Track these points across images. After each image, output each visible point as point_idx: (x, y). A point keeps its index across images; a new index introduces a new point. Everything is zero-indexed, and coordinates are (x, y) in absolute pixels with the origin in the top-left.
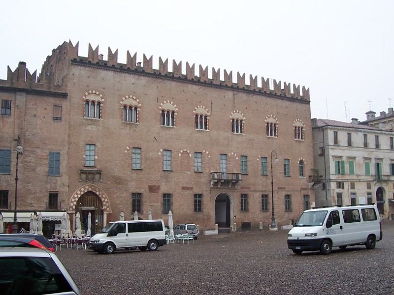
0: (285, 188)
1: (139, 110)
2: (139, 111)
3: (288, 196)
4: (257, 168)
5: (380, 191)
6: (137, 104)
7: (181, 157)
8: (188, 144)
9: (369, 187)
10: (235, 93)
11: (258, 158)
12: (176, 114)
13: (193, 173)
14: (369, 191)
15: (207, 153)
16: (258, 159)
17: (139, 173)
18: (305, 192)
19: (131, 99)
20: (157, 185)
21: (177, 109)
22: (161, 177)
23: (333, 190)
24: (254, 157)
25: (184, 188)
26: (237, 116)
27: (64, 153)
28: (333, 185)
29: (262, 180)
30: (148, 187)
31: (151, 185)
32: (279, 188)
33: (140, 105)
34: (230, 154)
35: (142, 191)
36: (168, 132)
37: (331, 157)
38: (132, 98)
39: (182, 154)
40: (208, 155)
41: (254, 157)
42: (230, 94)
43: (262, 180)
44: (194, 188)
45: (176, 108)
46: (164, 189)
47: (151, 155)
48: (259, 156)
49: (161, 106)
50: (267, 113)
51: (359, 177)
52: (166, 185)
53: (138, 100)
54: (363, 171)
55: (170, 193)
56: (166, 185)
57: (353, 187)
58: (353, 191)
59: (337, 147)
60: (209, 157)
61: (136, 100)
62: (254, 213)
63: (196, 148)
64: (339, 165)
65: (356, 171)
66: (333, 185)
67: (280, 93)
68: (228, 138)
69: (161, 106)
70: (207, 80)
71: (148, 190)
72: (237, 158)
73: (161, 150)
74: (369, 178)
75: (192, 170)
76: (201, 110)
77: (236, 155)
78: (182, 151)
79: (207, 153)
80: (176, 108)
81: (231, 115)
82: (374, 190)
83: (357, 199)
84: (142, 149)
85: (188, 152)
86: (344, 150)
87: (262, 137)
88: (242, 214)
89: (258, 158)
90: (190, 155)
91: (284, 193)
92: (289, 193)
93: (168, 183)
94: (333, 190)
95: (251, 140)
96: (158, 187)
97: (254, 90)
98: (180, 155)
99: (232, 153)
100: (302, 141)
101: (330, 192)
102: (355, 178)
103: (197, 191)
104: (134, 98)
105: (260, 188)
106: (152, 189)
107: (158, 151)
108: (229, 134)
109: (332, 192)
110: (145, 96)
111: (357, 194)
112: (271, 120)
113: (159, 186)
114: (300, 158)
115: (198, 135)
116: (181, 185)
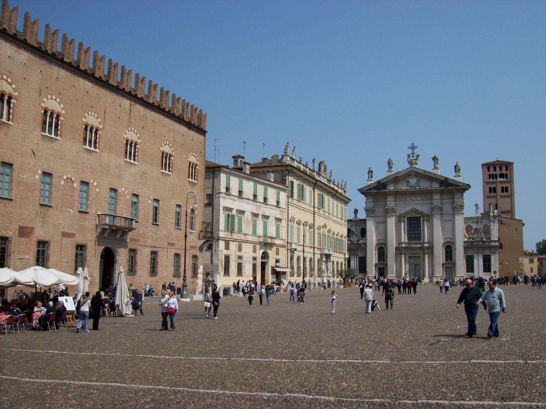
1: (15, 101)
2: (14, 103)
4: (149, 213)
5: (265, 256)
6: (12, 92)
7: (64, 185)
8: (73, 168)
9: (255, 251)
11: (150, 199)
12: (62, 118)
13: (78, 213)
14: (255, 255)
15: (95, 184)
17: (7, 205)
19: (4, 82)
20: (29, 225)
21: (64, 112)
22: (37, 214)
23: (222, 251)
24: (146, 197)
25: (64, 235)
26: (132, 136)
28: (222, 244)
29: (152, 231)
30: (18, 227)
31: (24, 225)
33: (16, 94)
34: (120, 190)
35: (9, 234)
36: (50, 145)
37: (221, 208)
38: (6, 80)
39: (65, 181)
40: (97, 186)
41: (146, 197)
43: (152, 231)
44: (77, 235)
45: (62, 109)
46: (40, 234)
47: (25, 177)
48: (152, 197)
49: (44, 102)
51: (247, 236)
52: (42, 227)
53: (14, 86)
54: (250, 231)
55: (47, 239)
56: (42, 227)
57: (240, 249)
58: (239, 254)
59: (228, 197)
60: (97, 190)
61: (10, 84)
62: (142, 276)
63: (82, 176)
64: (230, 219)
65: (244, 230)
66: (222, 244)
68: (120, 165)
69: (44, 102)
70: (102, 77)
71: (17, 233)
72: (128, 197)
73: (40, 172)
74: (255, 239)
75: (76, 208)
76: (92, 120)
77: (127, 192)
78: (65, 177)
79: (95, 184)
80: (62, 109)
81: (126, 133)
82: (259, 253)
83: (243, 264)
84: (14, 167)
85: (73, 179)
86: (235, 200)
87: (156, 170)
88: (128, 277)
89: (150, 199)
90: (75, 185)
91: (173, 251)
93: (45, 225)
94: (222, 251)
95: (144, 173)
96: (32, 229)
97: (153, 103)
98: (63, 182)
99: (123, 189)
101: (218, 254)
102: (243, 237)
103: (80, 240)
104: (9, 80)
105: (150, 242)
106: (24, 232)
107: (35, 173)
108: (121, 160)
109: (220, 254)
110: (24, 81)
111: (244, 258)
112: (167, 149)
113: (34, 228)
115: (85, 155)
116: (62, 230)
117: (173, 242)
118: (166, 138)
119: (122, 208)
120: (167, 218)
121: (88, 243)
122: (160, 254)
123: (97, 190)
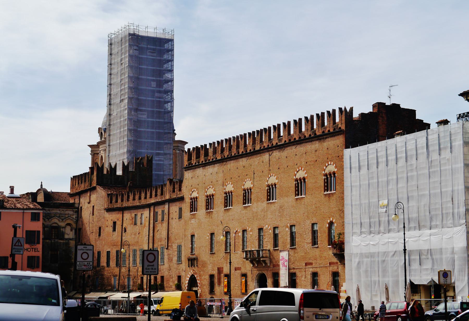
0: (311, 264)
3: (315, 275)
10: (271, 153)
15: (250, 229)
16: (287, 229)
18: (334, 268)
20: (221, 266)
24: (284, 226)
26: (273, 180)
27: (183, 244)
32: (306, 264)
34: (265, 228)
40: (251, 231)
41: (284, 226)
42: (266, 157)
44: (242, 268)
48: (288, 225)
50: (296, 166)
60: (251, 233)
67: (309, 133)
79: (250, 229)
89: (287, 226)
91: (310, 270)
92: (315, 270)
96: (223, 268)
99: (267, 226)
100: (332, 194)
103: (243, 271)
108: (265, 204)
114: (330, 218)
115: (244, 211)
117: (311, 261)
118: (298, 165)
119: (267, 241)
120: (304, 239)
121: (248, 272)
122: (298, 274)
123: (251, 233)
